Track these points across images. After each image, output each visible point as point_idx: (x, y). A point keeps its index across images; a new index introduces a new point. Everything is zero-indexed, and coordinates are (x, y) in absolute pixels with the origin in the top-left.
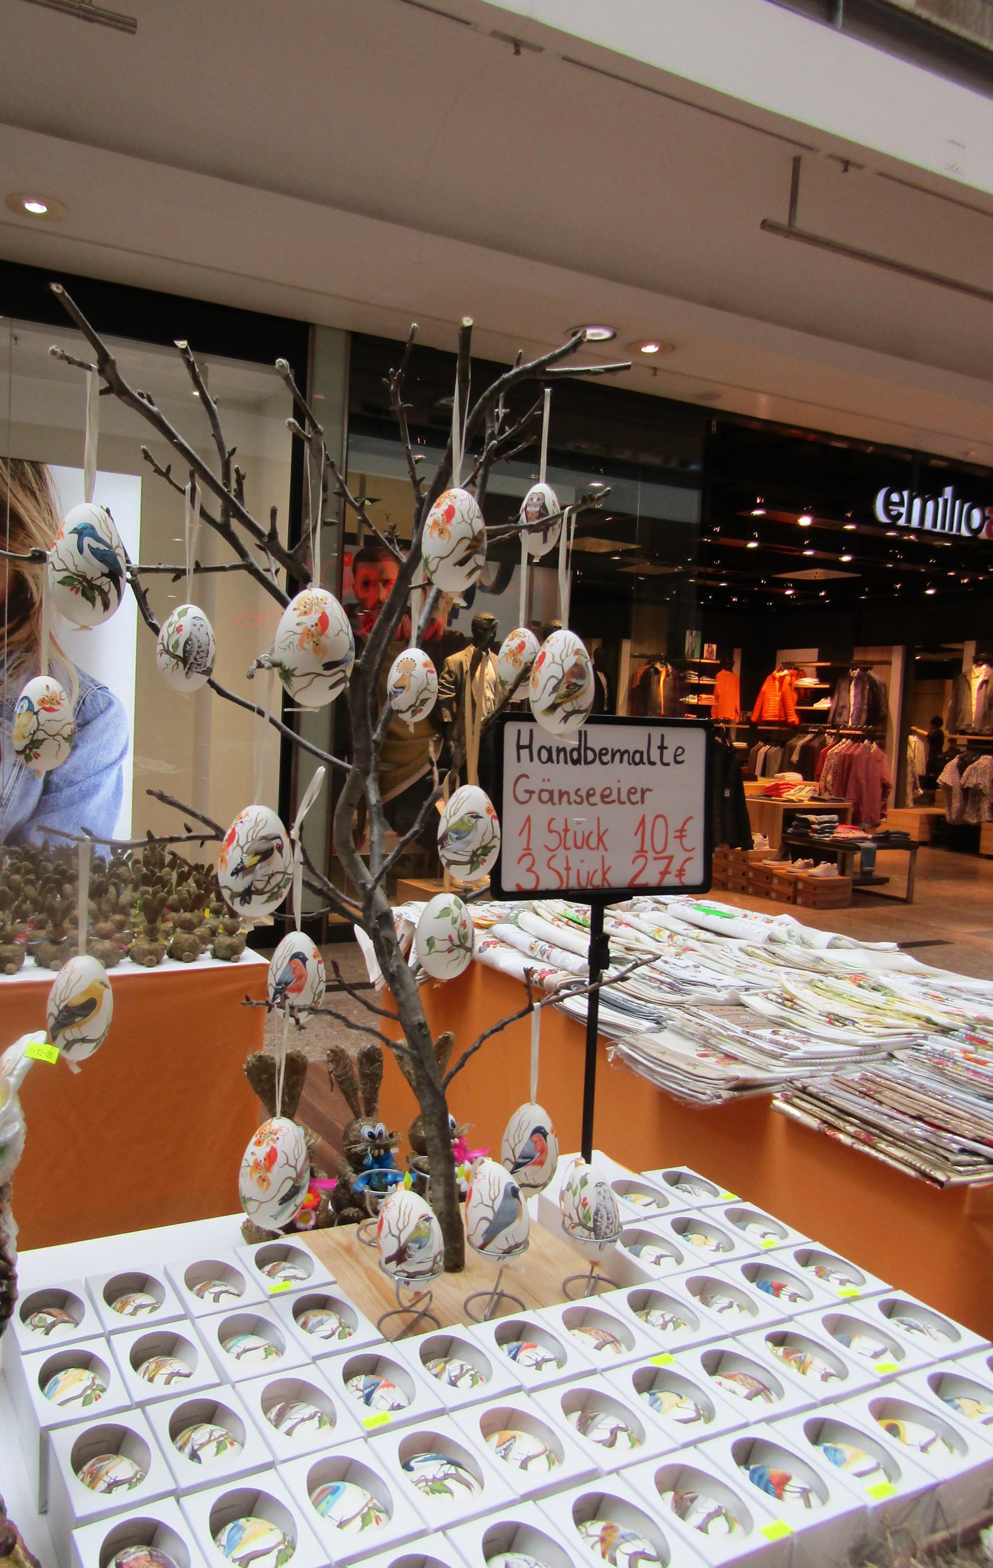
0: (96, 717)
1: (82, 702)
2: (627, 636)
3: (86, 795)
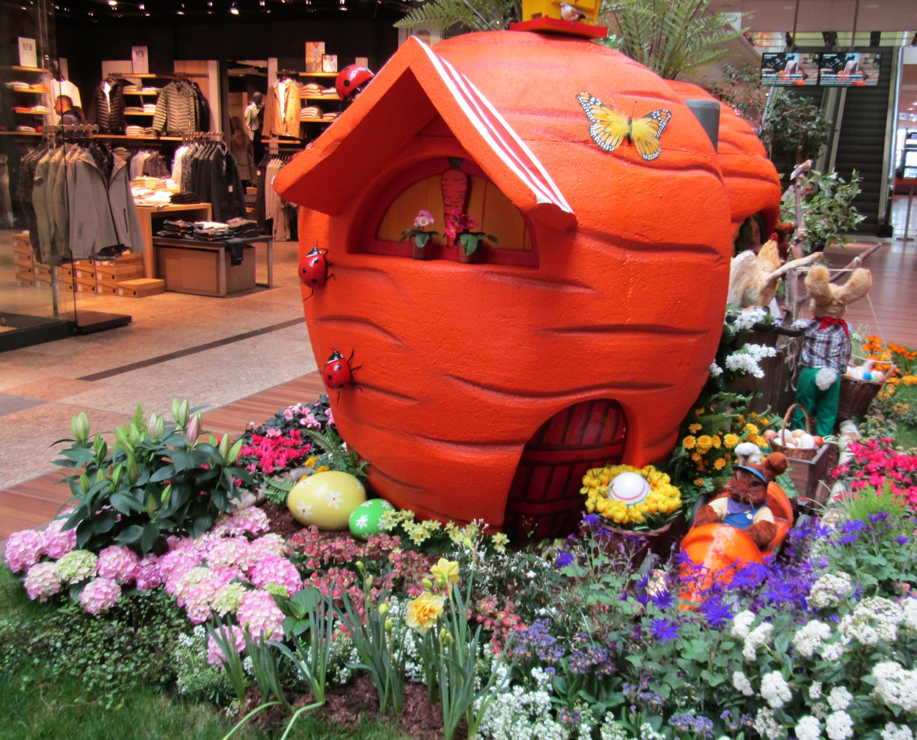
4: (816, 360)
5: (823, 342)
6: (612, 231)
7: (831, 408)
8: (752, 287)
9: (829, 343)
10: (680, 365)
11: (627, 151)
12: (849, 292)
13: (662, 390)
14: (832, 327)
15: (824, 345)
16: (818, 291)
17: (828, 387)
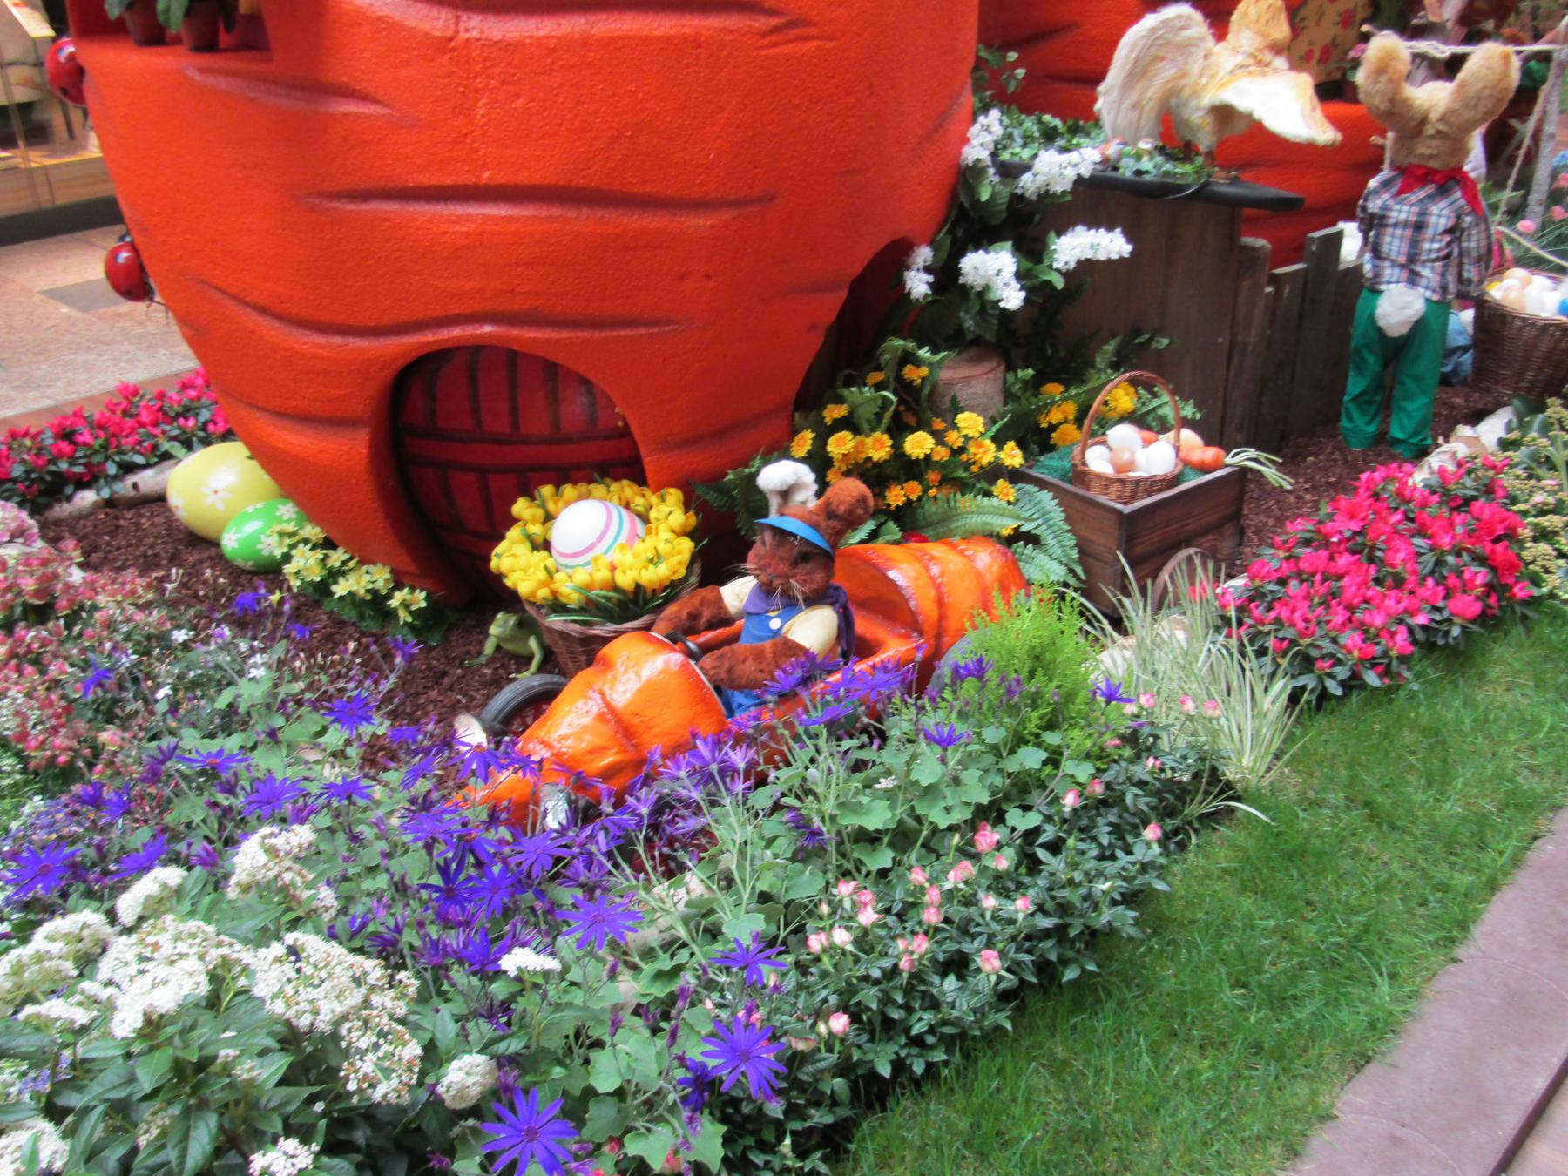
4: (1388, 272)
5: (1405, 224)
7: (1418, 379)
8: (1187, 92)
9: (1419, 227)
10: (682, 278)
12: (1457, 106)
13: (643, 331)
14: (1430, 189)
15: (1408, 233)
16: (1377, 101)
17: (1405, 330)
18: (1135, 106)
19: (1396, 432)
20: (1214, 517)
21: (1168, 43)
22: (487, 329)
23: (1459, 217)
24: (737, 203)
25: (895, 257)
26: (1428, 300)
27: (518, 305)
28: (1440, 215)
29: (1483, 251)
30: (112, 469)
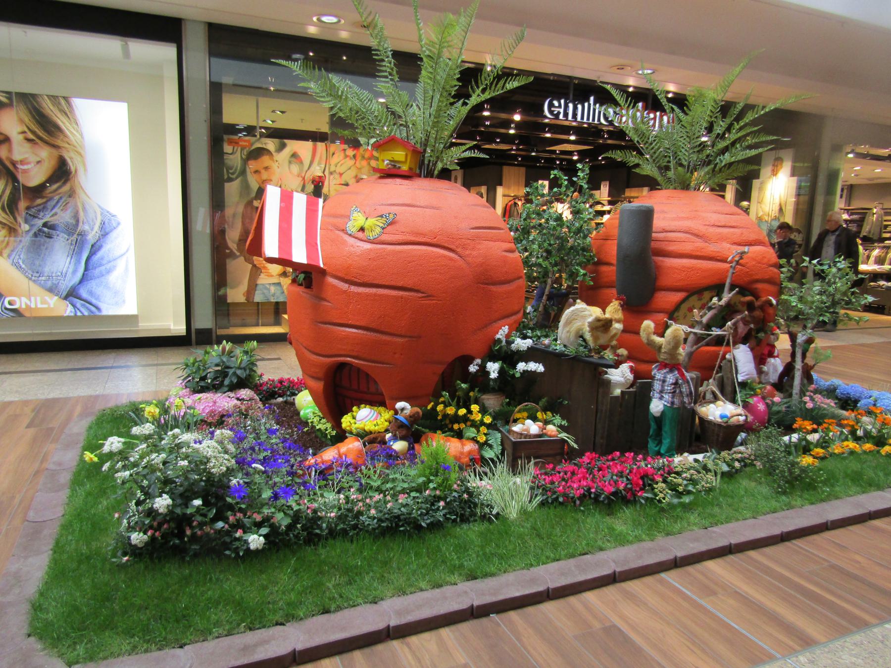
0: (111, 231)
1: (103, 223)
2: (501, 184)
3: (109, 272)
6: (340, 275)
9: (664, 381)
11: (360, 235)
14: (667, 370)
18: (568, 332)
19: (662, 451)
20: (551, 452)
21: (578, 315)
22: (349, 359)
23: (677, 380)
24: (410, 337)
25: (470, 360)
26: (665, 405)
27: (355, 354)
28: (671, 378)
29: (688, 393)
30: (288, 393)
